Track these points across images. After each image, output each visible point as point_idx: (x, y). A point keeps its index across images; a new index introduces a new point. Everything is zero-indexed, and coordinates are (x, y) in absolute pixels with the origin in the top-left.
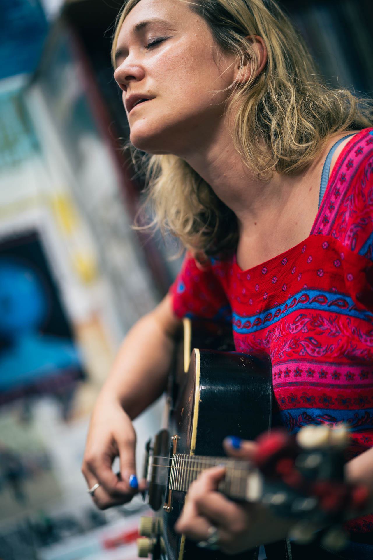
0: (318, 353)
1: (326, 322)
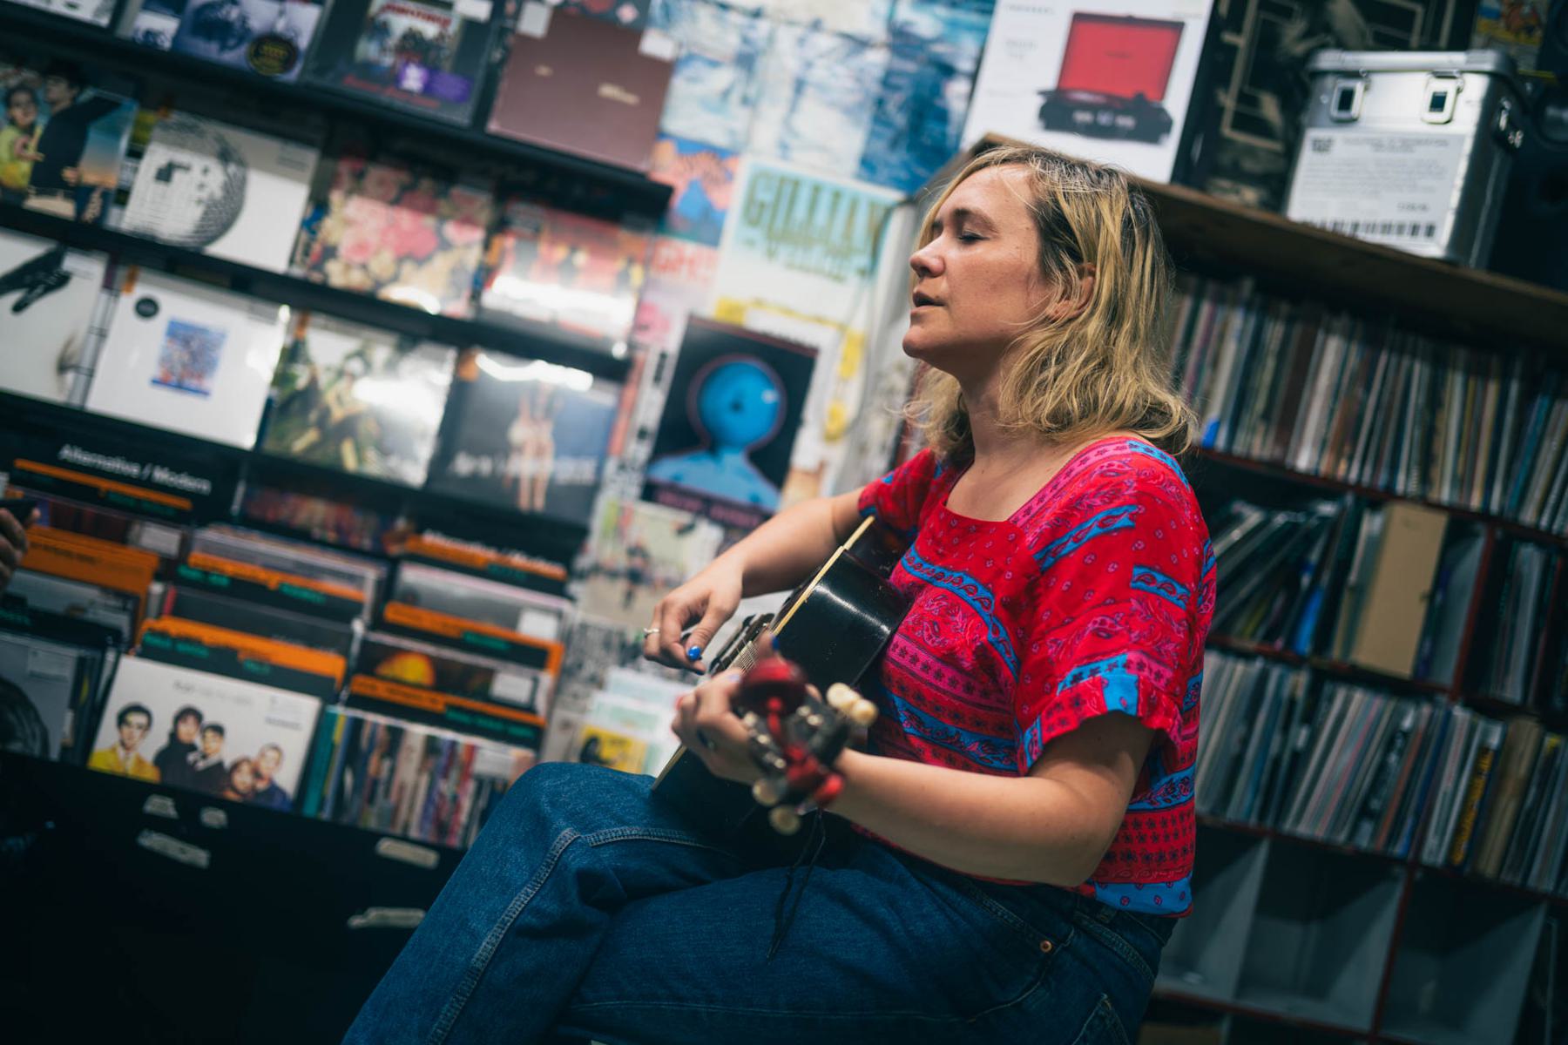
0: (933, 642)
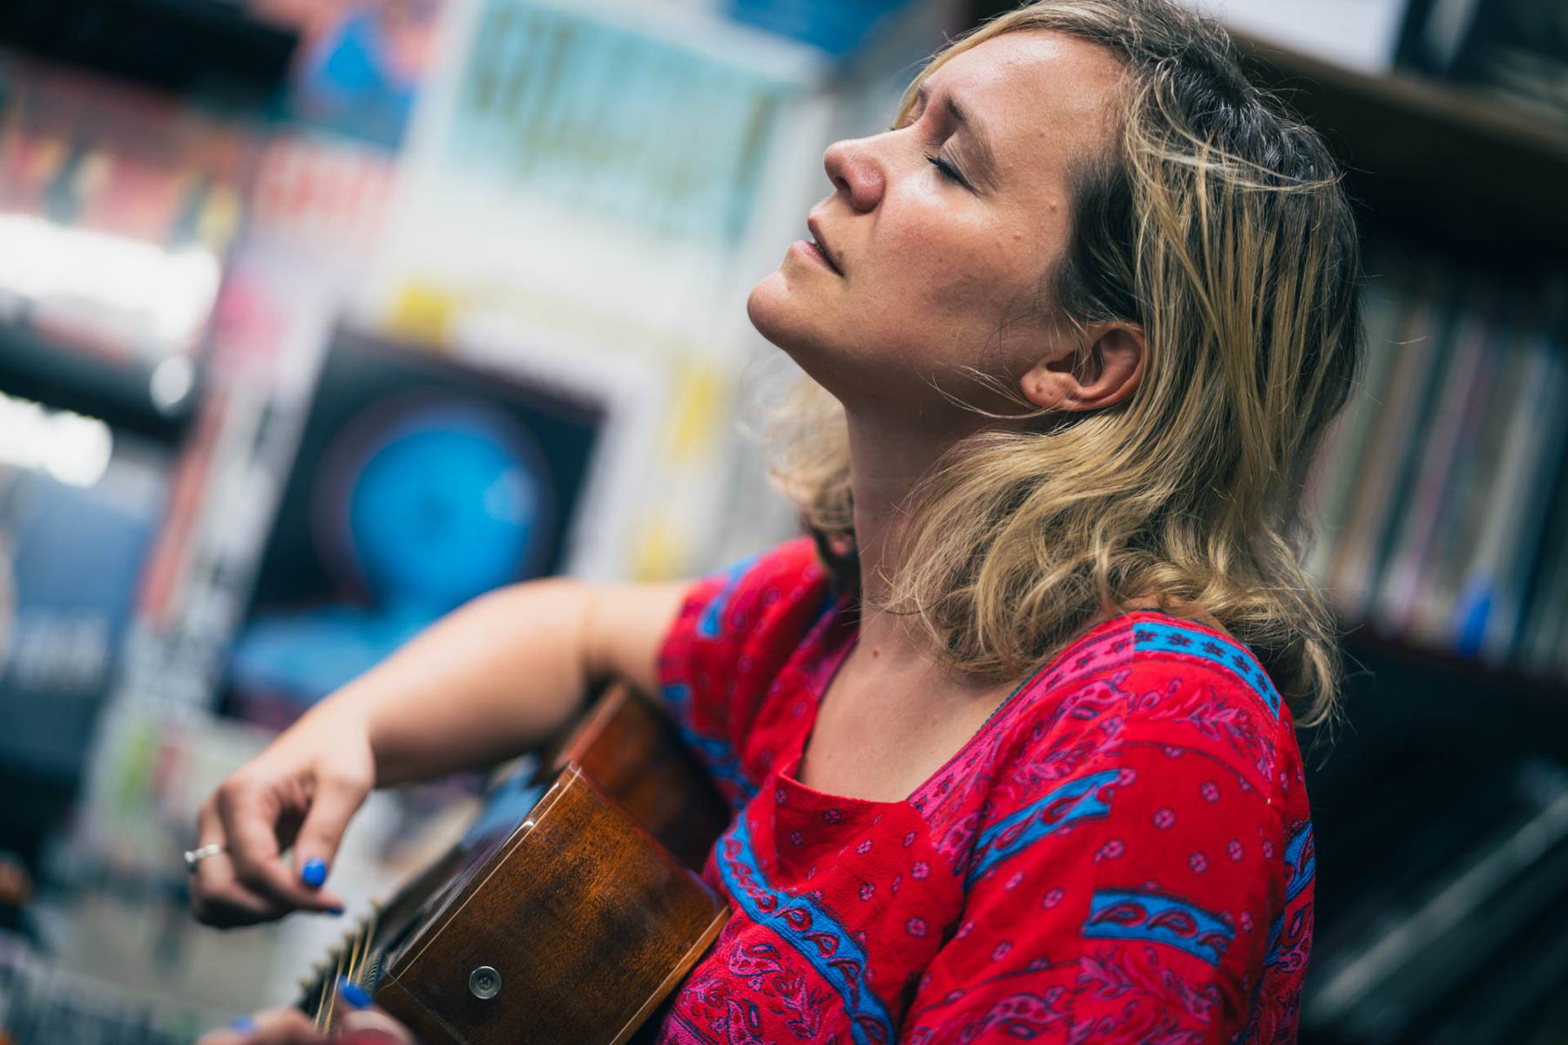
1: (802, 994)
